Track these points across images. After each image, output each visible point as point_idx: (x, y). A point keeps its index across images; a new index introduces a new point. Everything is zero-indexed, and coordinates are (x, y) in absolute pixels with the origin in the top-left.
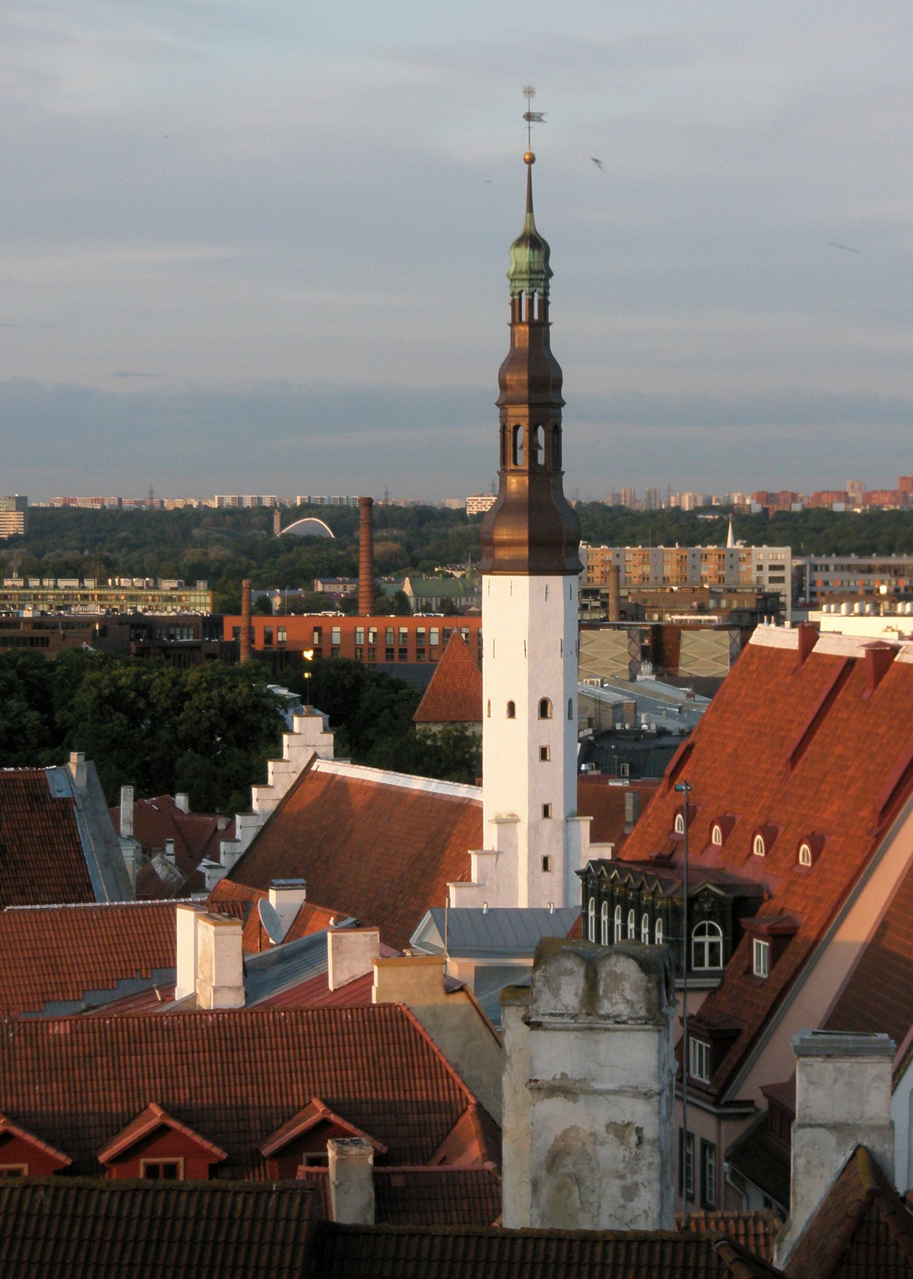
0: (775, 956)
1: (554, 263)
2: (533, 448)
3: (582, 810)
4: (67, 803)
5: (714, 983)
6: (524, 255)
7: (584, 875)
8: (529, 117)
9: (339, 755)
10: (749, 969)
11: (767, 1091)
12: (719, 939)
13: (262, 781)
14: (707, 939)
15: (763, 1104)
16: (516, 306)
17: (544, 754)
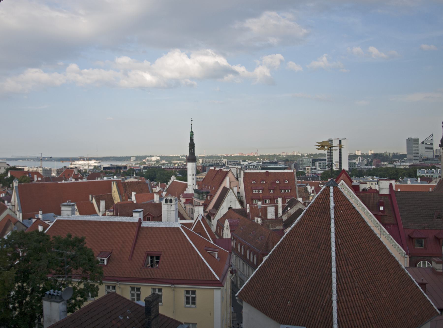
0: (210, 198)
1: (194, 134)
2: (192, 152)
3: (197, 184)
4: (147, 184)
5: (205, 200)
6: (191, 133)
7: (194, 190)
8: (192, 121)
9: (176, 179)
10: (208, 199)
11: (209, 210)
12: (205, 196)
13: (169, 182)
14: (204, 196)
15: (209, 211)
16: (190, 138)
17: (193, 179)
